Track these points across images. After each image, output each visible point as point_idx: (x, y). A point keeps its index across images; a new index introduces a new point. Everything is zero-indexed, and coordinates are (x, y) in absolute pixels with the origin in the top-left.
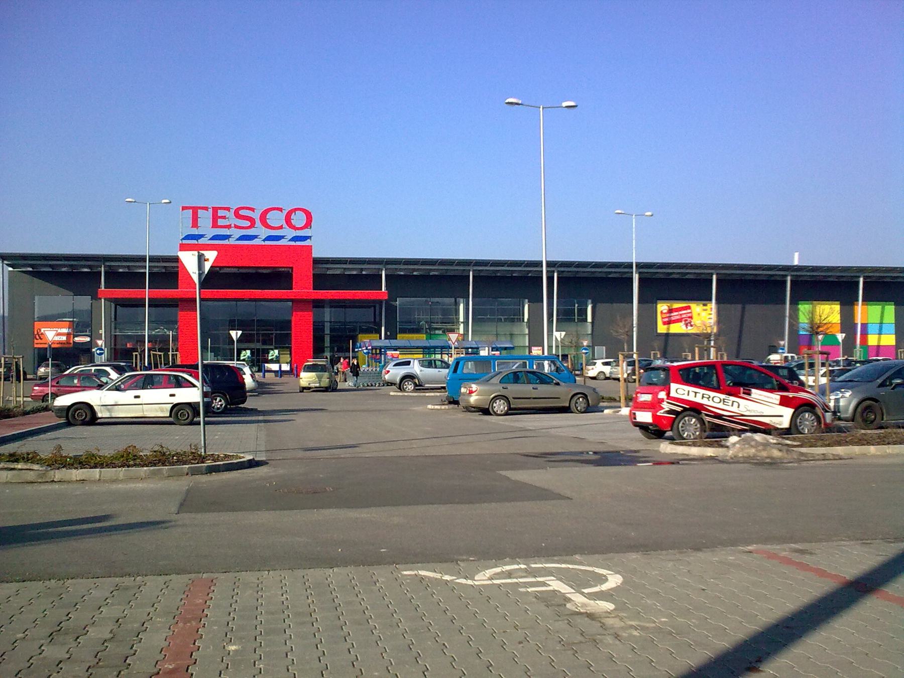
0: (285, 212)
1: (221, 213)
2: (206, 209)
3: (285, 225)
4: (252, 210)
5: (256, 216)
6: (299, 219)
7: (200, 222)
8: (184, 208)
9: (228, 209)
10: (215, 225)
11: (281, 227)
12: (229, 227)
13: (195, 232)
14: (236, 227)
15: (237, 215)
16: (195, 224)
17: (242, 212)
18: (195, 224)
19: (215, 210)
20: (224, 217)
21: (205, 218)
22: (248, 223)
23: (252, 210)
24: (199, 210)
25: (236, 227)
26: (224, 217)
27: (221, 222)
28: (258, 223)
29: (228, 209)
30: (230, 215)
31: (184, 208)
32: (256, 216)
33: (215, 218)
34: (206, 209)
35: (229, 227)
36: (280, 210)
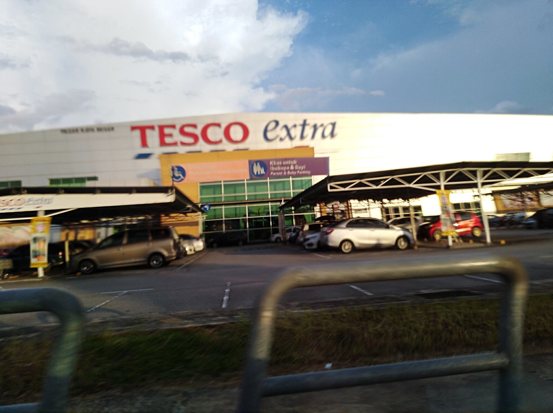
0: (224, 126)
1: (167, 131)
2: (152, 128)
3: (225, 141)
4: (195, 126)
5: (198, 132)
6: (236, 133)
7: (149, 141)
8: (133, 128)
9: (173, 127)
10: (163, 143)
11: (220, 141)
12: (175, 144)
13: (145, 151)
14: (183, 144)
15: (182, 132)
16: (144, 143)
17: (187, 130)
18: (144, 143)
19: (161, 128)
20: (170, 135)
21: (153, 137)
22: (190, 140)
23: (195, 126)
24: (148, 132)
25: (183, 144)
26: (170, 135)
27: (168, 140)
28: (201, 140)
29: (173, 127)
30: (176, 132)
31: (133, 128)
32: (198, 132)
33: (162, 135)
34: (152, 128)
35: (175, 144)
36: (219, 125)
